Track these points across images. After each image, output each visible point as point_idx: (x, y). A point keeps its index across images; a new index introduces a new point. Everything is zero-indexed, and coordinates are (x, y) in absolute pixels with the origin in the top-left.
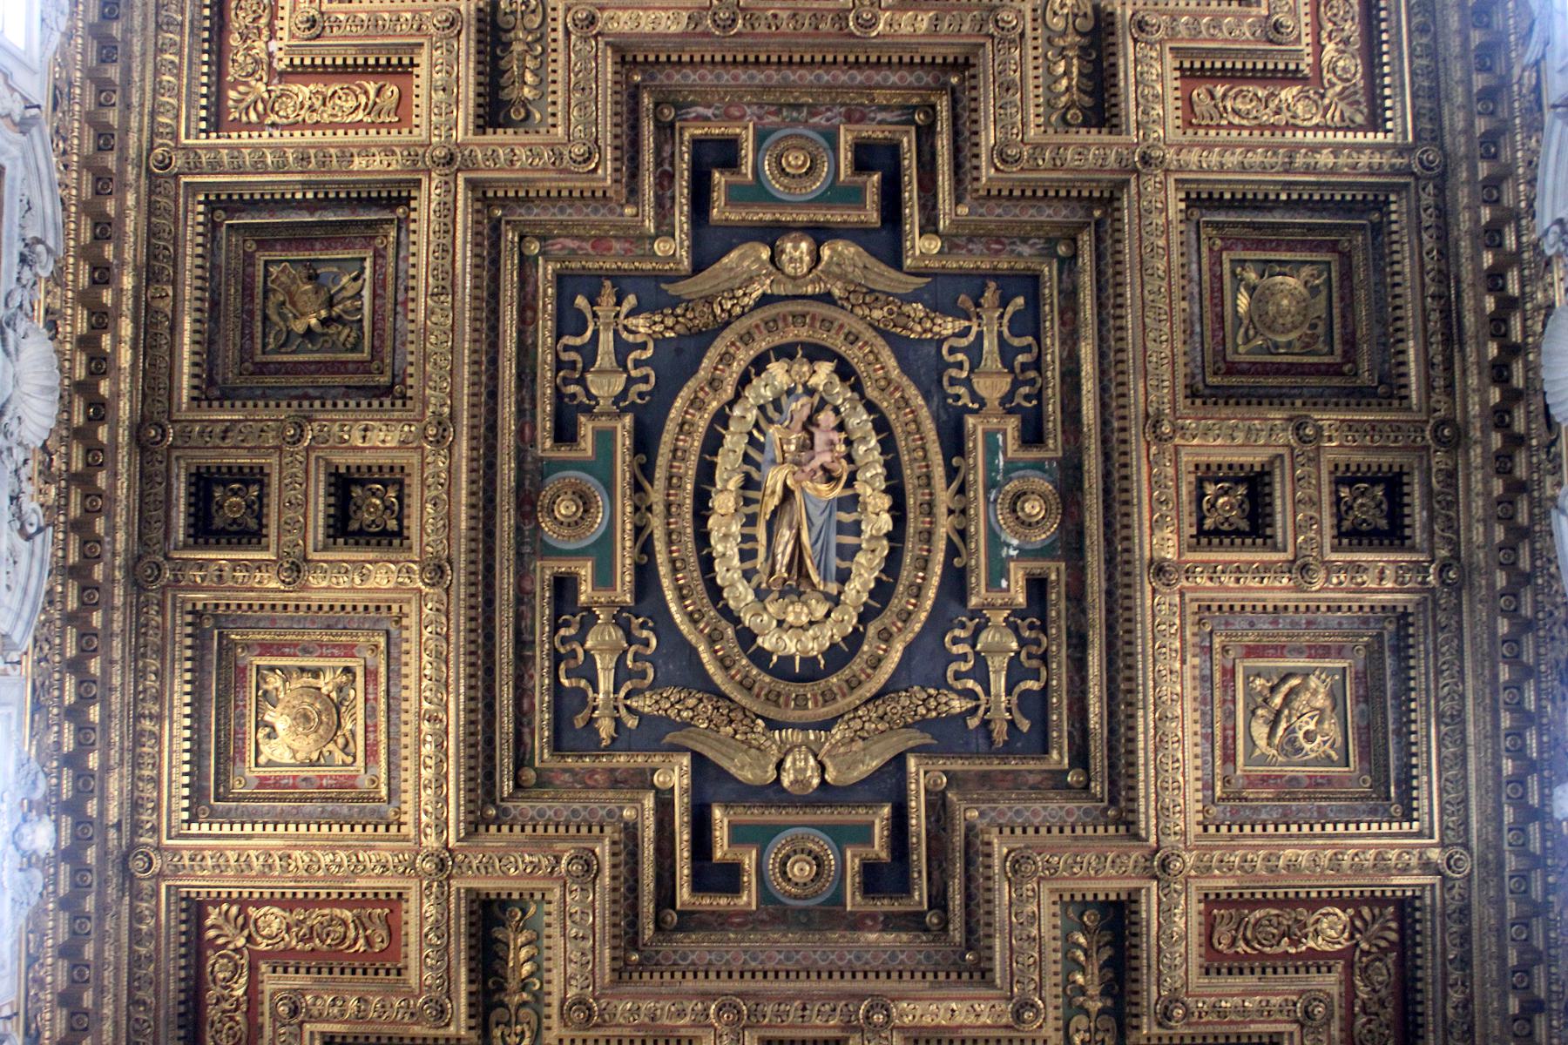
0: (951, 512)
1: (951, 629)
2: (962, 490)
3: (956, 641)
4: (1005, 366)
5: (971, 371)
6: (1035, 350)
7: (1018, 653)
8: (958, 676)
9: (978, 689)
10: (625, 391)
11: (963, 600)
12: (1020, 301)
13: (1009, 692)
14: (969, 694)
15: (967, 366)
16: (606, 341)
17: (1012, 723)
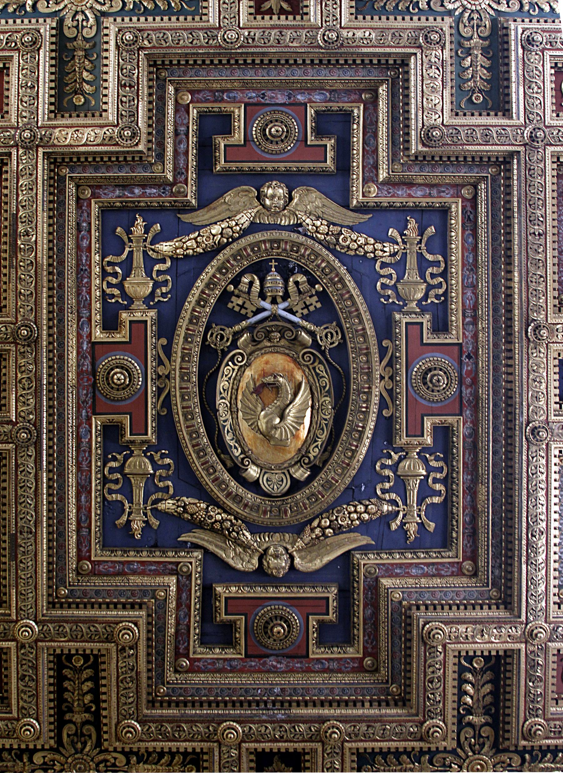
0: (382, 378)
1: (380, 458)
2: (390, 364)
3: (383, 466)
4: (421, 278)
5: (398, 281)
6: (443, 265)
7: (427, 477)
8: (384, 491)
9: (398, 500)
10: (153, 293)
11: (390, 441)
12: (431, 230)
13: (419, 503)
14: (393, 502)
15: (394, 276)
16: (138, 259)
17: (421, 525)
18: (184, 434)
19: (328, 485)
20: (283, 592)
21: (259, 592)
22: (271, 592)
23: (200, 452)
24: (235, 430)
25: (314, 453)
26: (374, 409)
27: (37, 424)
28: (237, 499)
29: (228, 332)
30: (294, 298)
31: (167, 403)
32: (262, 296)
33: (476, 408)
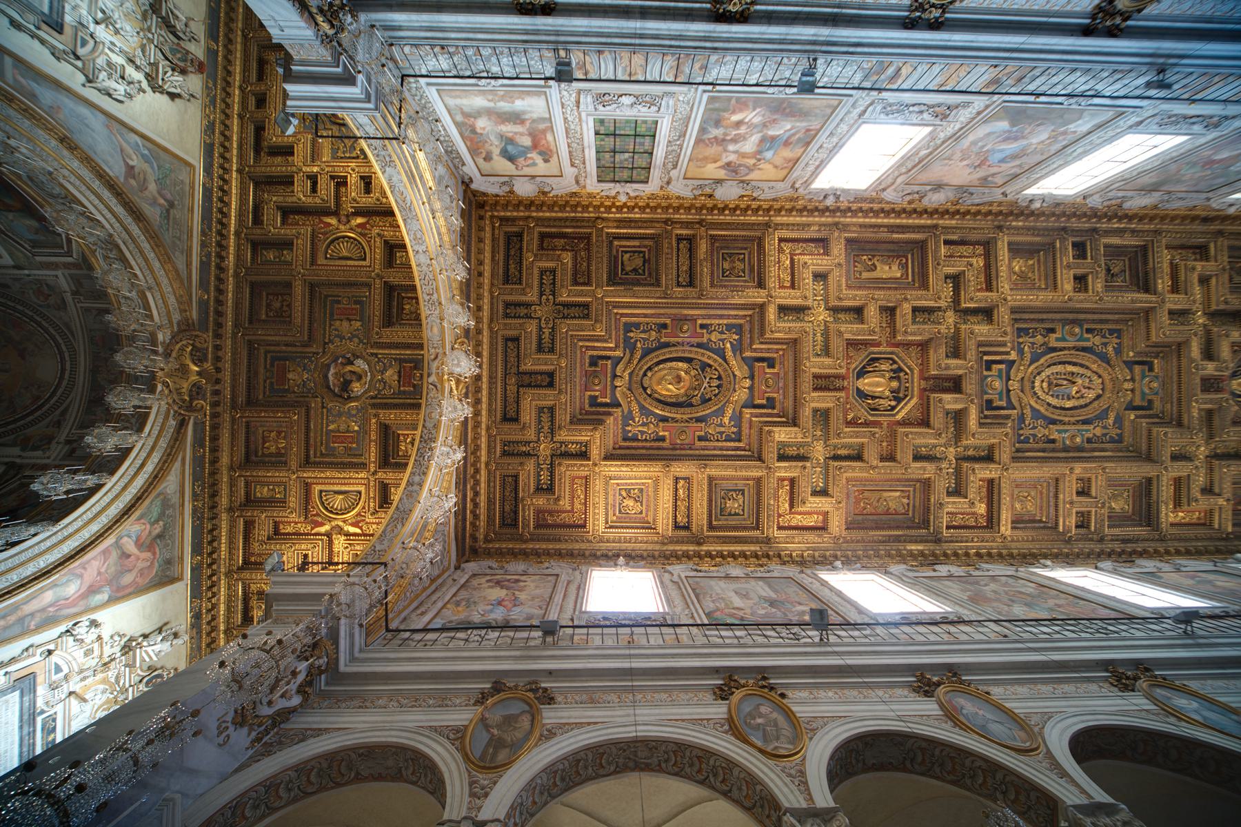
18: (664, 350)
19: (645, 400)
20: (609, 383)
21: (609, 375)
22: (609, 379)
23: (657, 356)
24: (664, 368)
25: (656, 395)
26: (672, 415)
27: (671, 298)
28: (641, 369)
29: (698, 367)
30: (709, 389)
31: (674, 345)
32: (711, 378)
33: (672, 449)
